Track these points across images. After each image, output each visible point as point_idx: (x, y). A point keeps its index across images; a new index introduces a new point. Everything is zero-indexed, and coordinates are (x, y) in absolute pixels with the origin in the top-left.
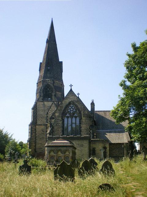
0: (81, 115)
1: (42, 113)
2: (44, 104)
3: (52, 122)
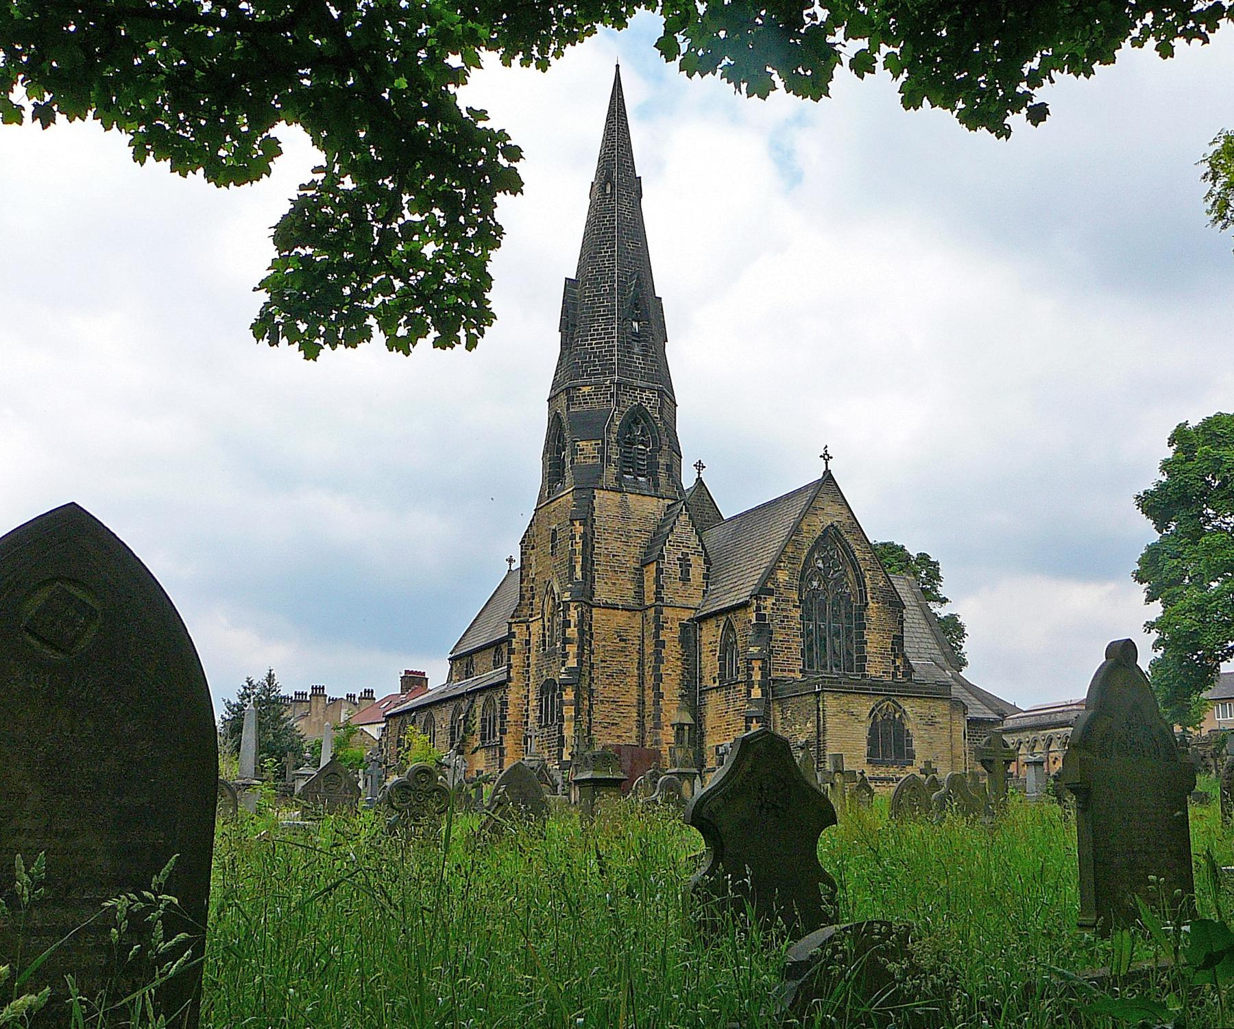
0: (865, 588)
1: (615, 546)
2: (623, 505)
3: (765, 608)
